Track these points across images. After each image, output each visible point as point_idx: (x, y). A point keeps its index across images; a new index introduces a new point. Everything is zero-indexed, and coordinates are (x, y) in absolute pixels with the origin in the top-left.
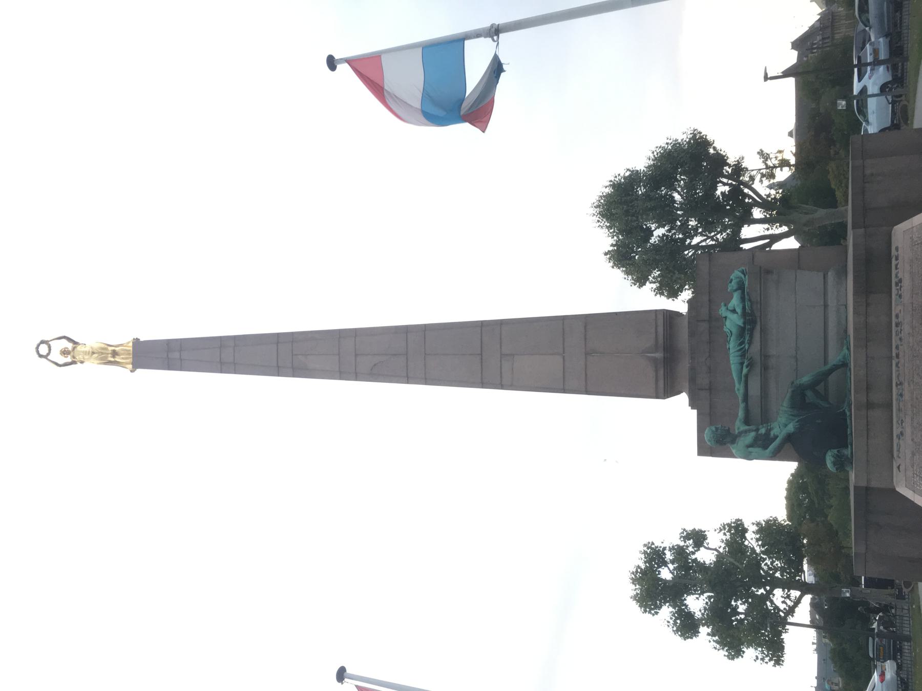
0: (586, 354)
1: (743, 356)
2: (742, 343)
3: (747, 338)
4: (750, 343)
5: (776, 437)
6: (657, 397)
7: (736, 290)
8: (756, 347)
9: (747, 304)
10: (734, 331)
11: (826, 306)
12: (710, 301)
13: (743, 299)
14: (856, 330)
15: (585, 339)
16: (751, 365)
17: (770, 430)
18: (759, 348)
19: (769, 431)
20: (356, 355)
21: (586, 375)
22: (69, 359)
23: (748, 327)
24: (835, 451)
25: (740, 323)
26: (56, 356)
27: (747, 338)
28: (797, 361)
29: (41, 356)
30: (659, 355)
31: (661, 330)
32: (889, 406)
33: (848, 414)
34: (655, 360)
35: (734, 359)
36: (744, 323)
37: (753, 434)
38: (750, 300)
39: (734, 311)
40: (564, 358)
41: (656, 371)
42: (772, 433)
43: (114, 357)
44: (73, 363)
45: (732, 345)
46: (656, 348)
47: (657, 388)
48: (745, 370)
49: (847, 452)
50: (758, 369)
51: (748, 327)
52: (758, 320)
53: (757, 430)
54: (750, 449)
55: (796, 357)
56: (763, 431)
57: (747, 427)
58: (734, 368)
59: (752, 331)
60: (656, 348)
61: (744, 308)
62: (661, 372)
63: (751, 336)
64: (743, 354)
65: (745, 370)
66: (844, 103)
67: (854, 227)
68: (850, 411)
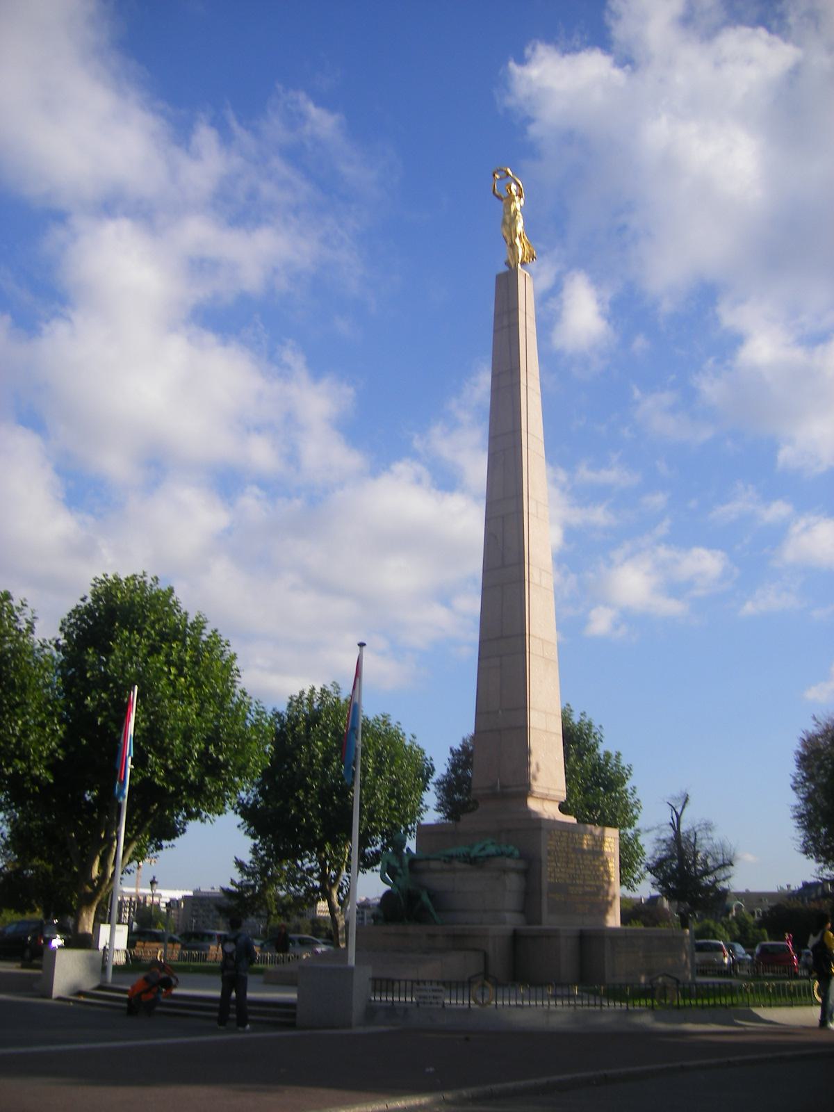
1: (457, 857)
19: (400, 875)
37: (397, 865)
46: (503, 787)
60: (503, 787)
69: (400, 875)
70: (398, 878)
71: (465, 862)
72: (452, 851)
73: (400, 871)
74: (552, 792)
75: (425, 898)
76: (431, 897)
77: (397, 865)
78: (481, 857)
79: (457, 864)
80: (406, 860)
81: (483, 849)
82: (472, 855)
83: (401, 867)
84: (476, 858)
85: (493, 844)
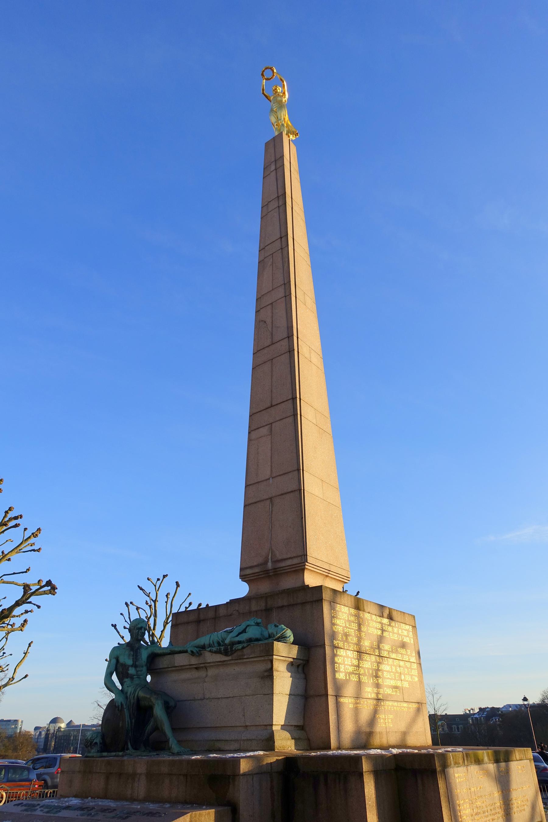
4: (210, 651)
6: (241, 569)
12: (283, 607)
15: (282, 494)
18: (209, 661)
19: (132, 677)
21: (255, 503)
23: (222, 648)
28: (201, 699)
31: (289, 563)
32: (105, 797)
34: (266, 563)
37: (129, 662)
38: (243, 648)
40: (269, 479)
47: (246, 568)
52: (230, 658)
54: (114, 661)
55: (204, 698)
62: (256, 570)
63: (216, 652)
69: (132, 677)
70: (127, 681)
71: (218, 652)
72: (204, 640)
73: (132, 671)
74: (333, 569)
75: (159, 711)
76: (169, 709)
77: (129, 662)
78: (239, 642)
79: (209, 657)
80: (144, 655)
81: (244, 631)
82: (227, 641)
83: (135, 666)
84: (233, 644)
85: (258, 624)
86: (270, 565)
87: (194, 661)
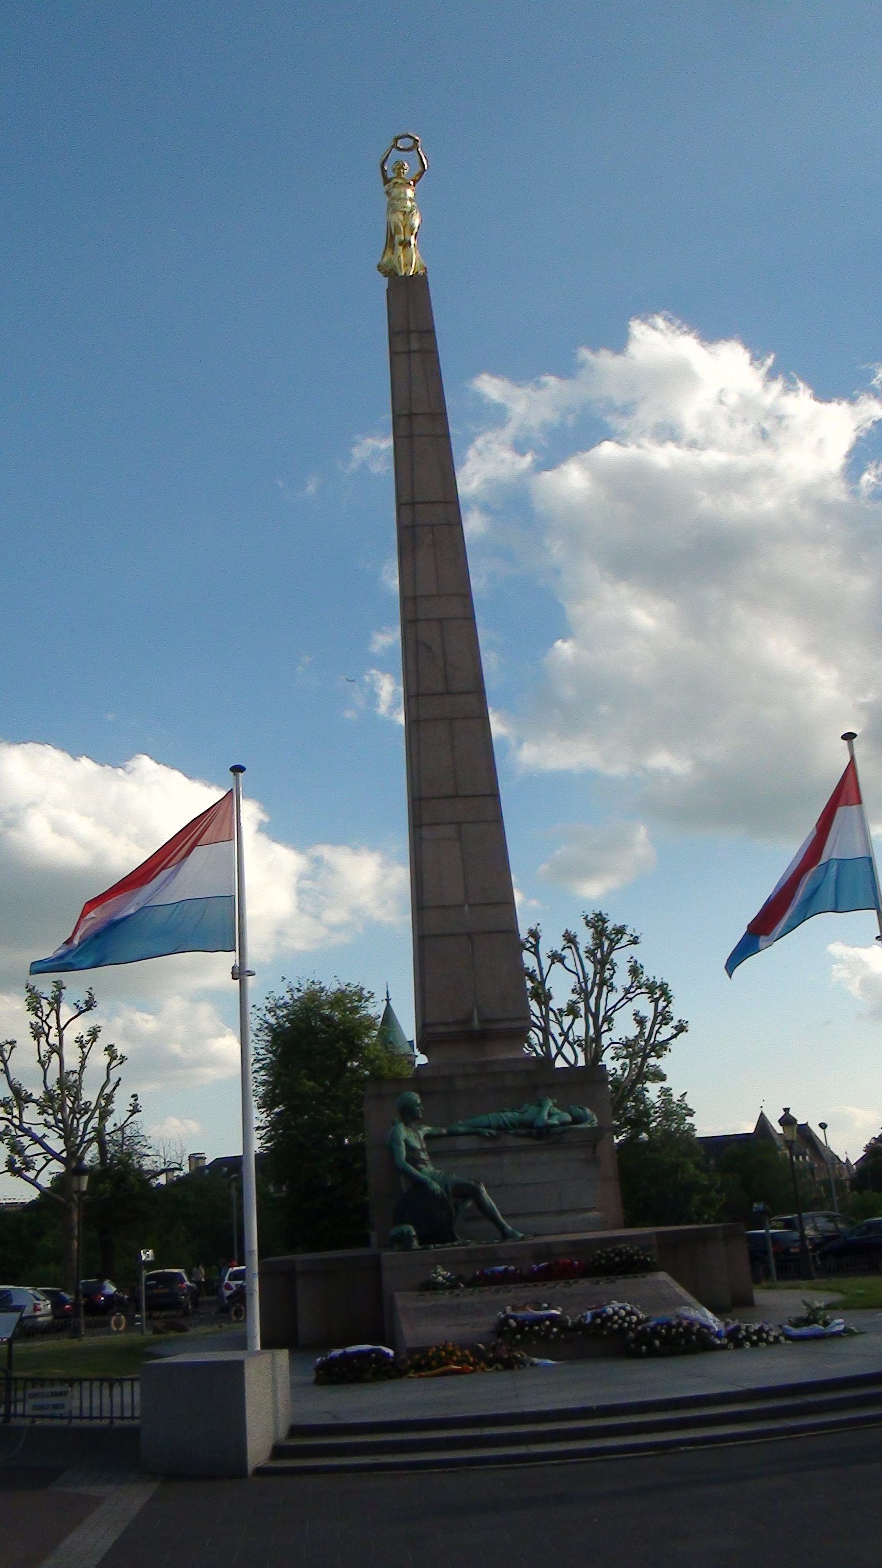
0: (469, 935)
2: (512, 1124)
3: (523, 1132)
5: (420, 1170)
7: (571, 1114)
8: (512, 1141)
9: (560, 1129)
10: (527, 1116)
11: (561, 1212)
13: (563, 1124)
14: (548, 1245)
16: (492, 1138)
17: (425, 1164)
20: (440, 620)
22: (390, 175)
24: (414, 1233)
25: (539, 1123)
26: (395, 155)
27: (523, 1132)
28: (499, 1186)
29: (396, 140)
30: (476, 1024)
31: (507, 1025)
33: (456, 1243)
34: (468, 1020)
35: (492, 1118)
36: (538, 1127)
37: (418, 1145)
39: (550, 1115)
41: (454, 1023)
42: (422, 1166)
43: (401, 243)
44: (386, 181)
45: (509, 1116)
48: (487, 1132)
49: (415, 1244)
50: (487, 1145)
51: (534, 1131)
53: (423, 1150)
54: (403, 1144)
56: (424, 1156)
57: (422, 1137)
58: (484, 1119)
59: (530, 1136)
61: (554, 1126)
62: (454, 1028)
63: (523, 1136)
64: (503, 1128)
65: (487, 1132)
66: (755, 1205)
67: (659, 1234)
68: (459, 1245)
86: (476, 1024)
87: (487, 1145)
